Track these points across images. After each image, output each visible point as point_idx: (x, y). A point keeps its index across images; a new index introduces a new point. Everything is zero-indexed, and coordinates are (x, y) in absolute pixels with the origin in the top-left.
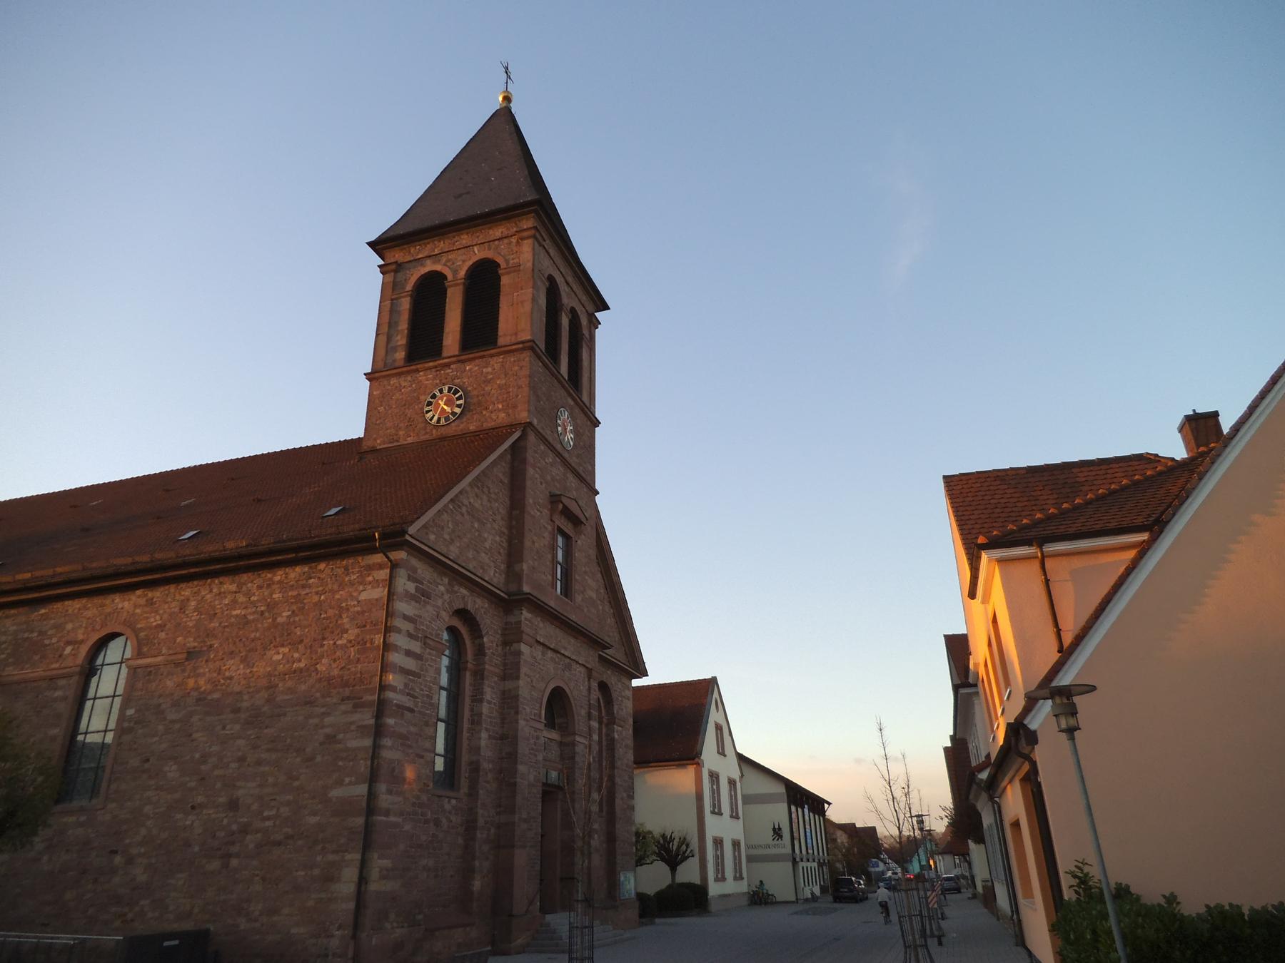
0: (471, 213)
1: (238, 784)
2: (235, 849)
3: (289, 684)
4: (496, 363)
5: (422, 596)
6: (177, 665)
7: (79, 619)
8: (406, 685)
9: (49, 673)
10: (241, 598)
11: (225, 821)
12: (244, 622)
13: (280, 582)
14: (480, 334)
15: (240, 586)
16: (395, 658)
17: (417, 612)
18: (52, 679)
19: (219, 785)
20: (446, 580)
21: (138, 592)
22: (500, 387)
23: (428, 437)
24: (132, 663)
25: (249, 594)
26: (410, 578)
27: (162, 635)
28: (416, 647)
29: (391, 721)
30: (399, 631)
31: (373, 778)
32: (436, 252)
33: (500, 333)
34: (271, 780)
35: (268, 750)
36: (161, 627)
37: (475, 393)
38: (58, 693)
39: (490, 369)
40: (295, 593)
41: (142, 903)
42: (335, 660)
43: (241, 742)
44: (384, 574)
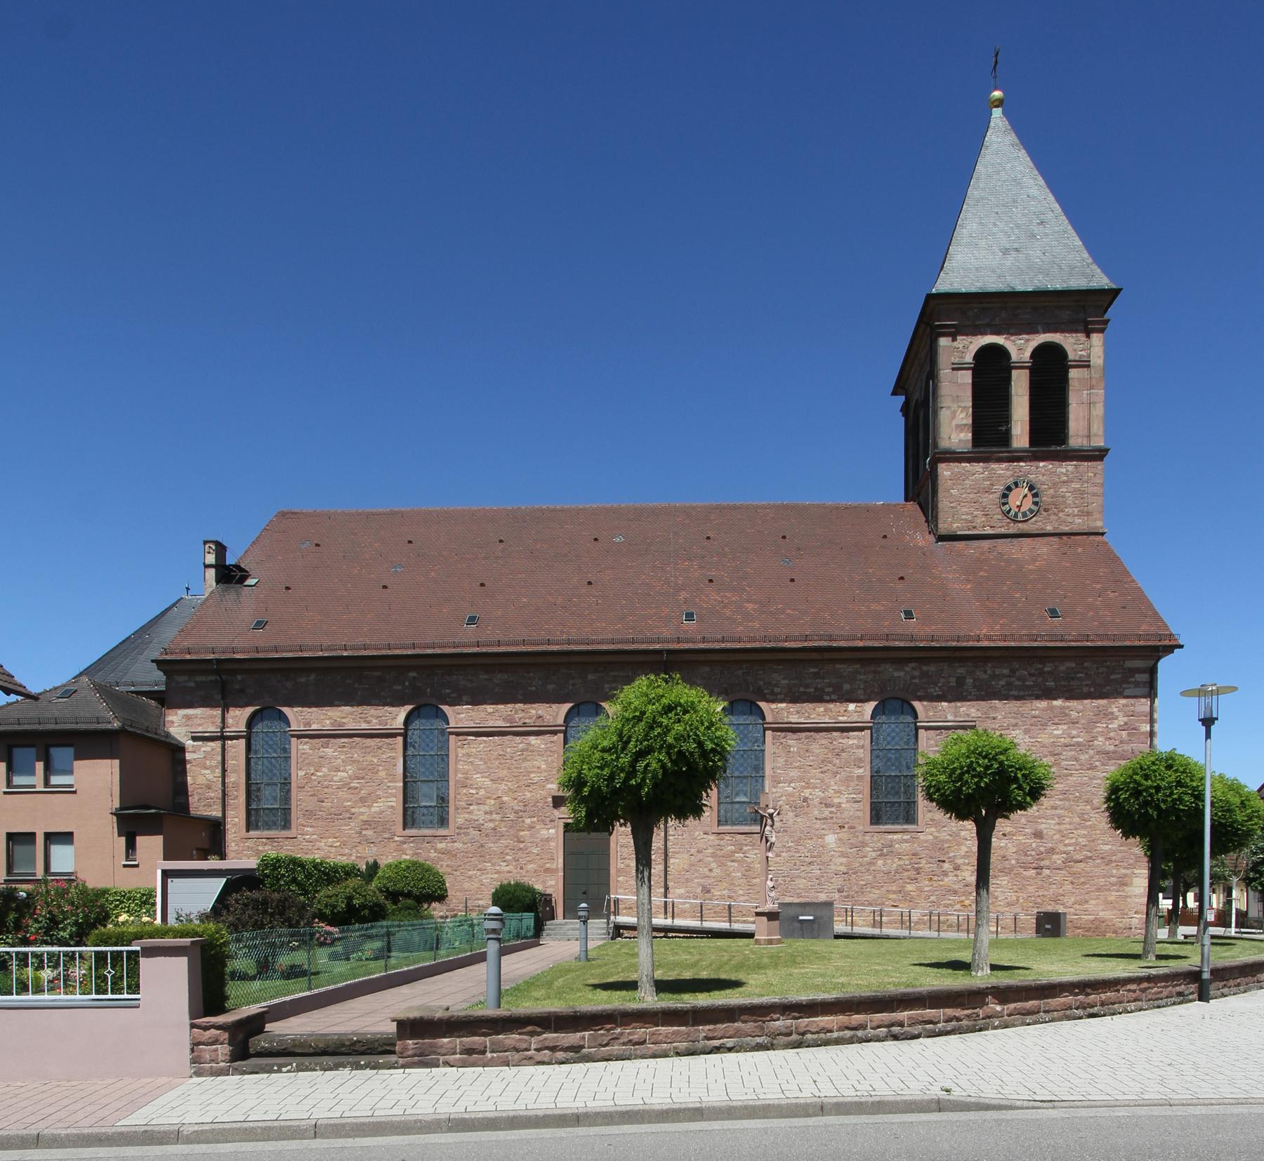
13: (1049, 673)
15: (1013, 671)
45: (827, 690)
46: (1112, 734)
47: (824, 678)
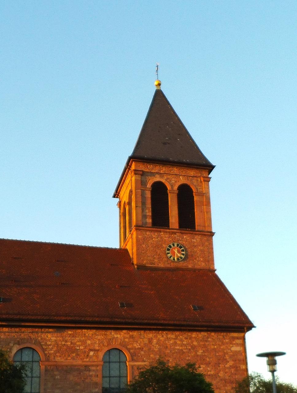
10: (178, 342)
21: (124, 331)
22: (201, 250)
23: (168, 266)
27: (142, 353)
36: (141, 349)
40: (203, 343)
45: (78, 343)
46: (227, 370)
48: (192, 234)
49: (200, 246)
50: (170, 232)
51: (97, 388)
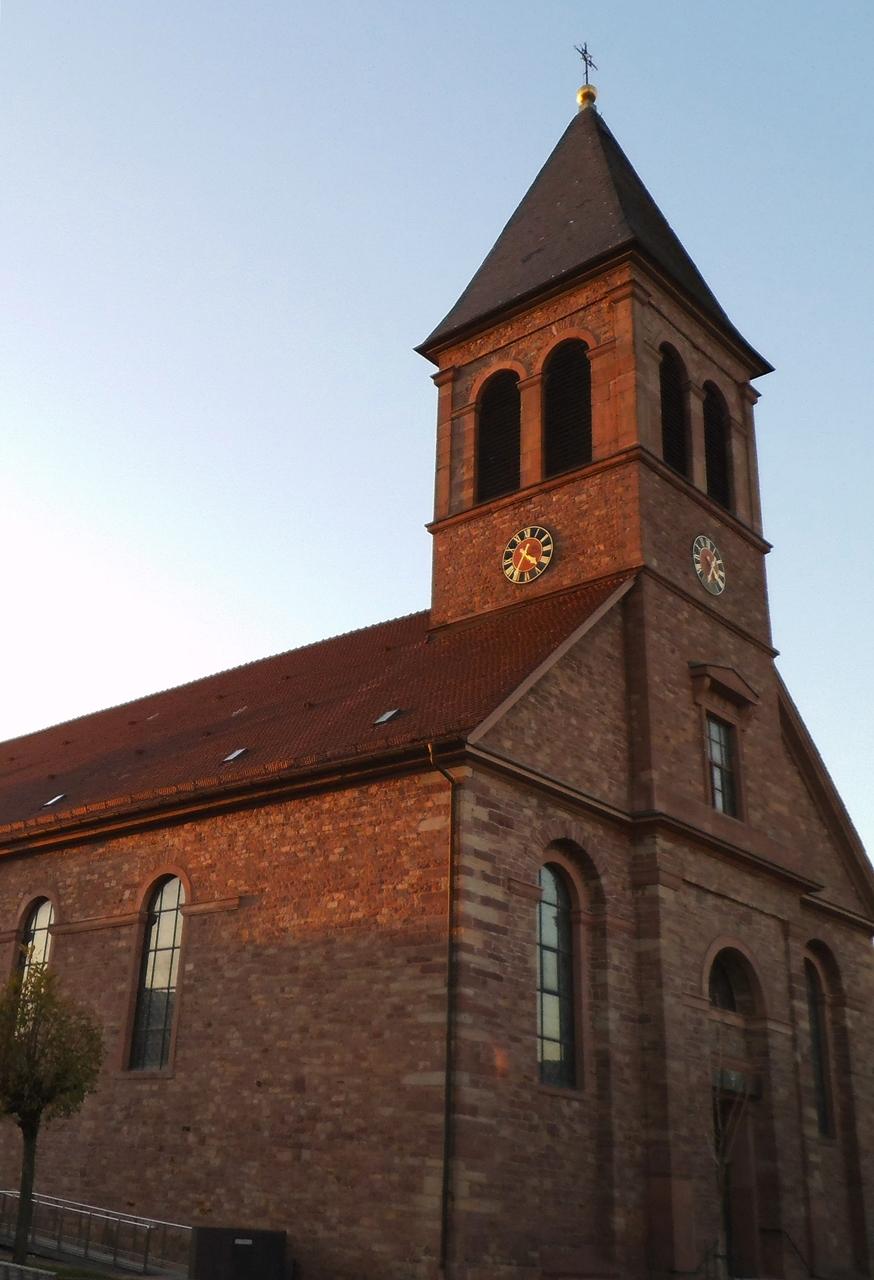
0: (543, 280)
1: (304, 1059)
2: (305, 1138)
3: (348, 939)
4: (591, 487)
5: (500, 824)
6: (231, 912)
7: (135, 855)
8: (487, 944)
9: (112, 921)
10: (290, 833)
11: (293, 1103)
12: (293, 862)
13: (329, 811)
14: (569, 448)
16: (468, 908)
17: (493, 847)
18: (115, 927)
19: (282, 1060)
20: (534, 801)
22: (599, 521)
24: (186, 909)
25: (297, 827)
26: (480, 802)
27: (213, 876)
28: (497, 893)
29: (469, 991)
30: (470, 872)
31: (451, 1065)
32: (503, 344)
33: (594, 442)
34: (336, 1057)
35: (331, 1021)
36: (211, 867)
37: (567, 533)
38: (122, 944)
39: (584, 496)
40: (346, 824)
41: (218, 1191)
42: (396, 910)
43: (301, 1009)
44: (444, 797)
46: (401, 901)
47: (108, 859)
48: (573, 480)
49: (597, 508)
50: (512, 504)
51: (123, 980)
